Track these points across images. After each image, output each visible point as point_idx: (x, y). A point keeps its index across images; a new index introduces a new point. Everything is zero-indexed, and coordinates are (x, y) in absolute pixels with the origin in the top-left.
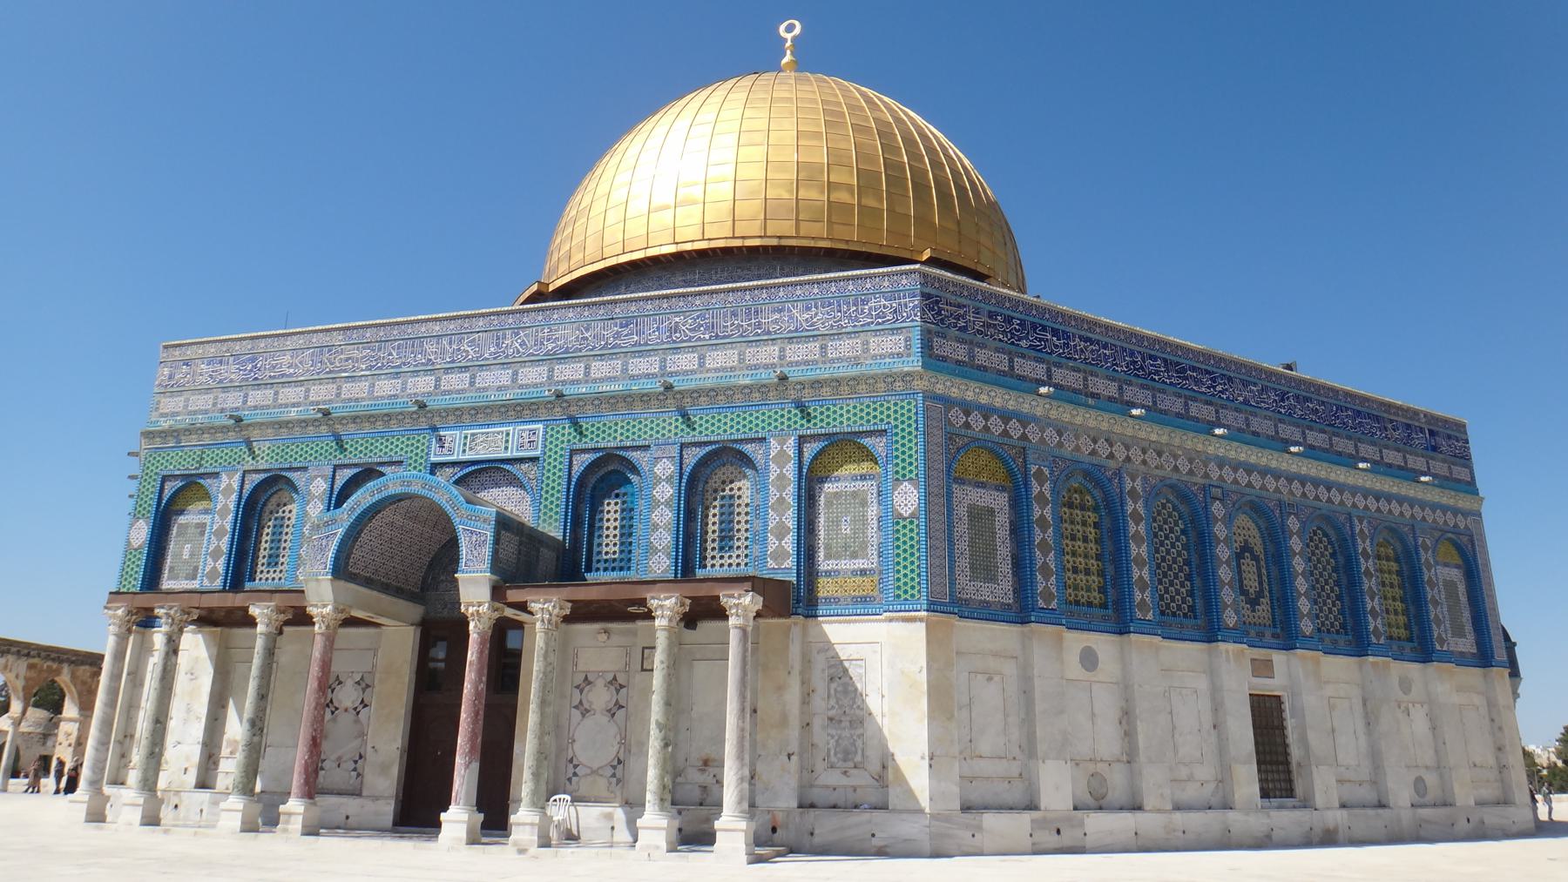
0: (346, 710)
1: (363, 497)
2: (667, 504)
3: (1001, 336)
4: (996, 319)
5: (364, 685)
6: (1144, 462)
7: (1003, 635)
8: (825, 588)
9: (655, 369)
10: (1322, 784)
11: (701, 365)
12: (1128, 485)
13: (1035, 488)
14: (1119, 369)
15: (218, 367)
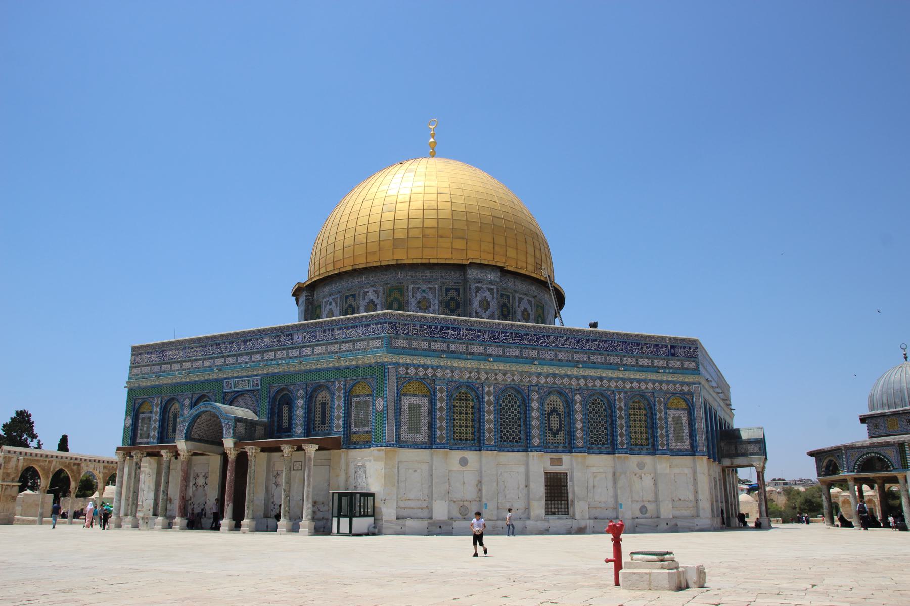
0: (200, 486)
1: (202, 406)
2: (302, 407)
3: (425, 334)
4: (423, 328)
5: (206, 477)
6: (496, 379)
7: (423, 454)
8: (355, 438)
9: (297, 354)
10: (580, 509)
11: (313, 352)
12: (486, 389)
13: (439, 395)
14: (486, 340)
15: (151, 355)
